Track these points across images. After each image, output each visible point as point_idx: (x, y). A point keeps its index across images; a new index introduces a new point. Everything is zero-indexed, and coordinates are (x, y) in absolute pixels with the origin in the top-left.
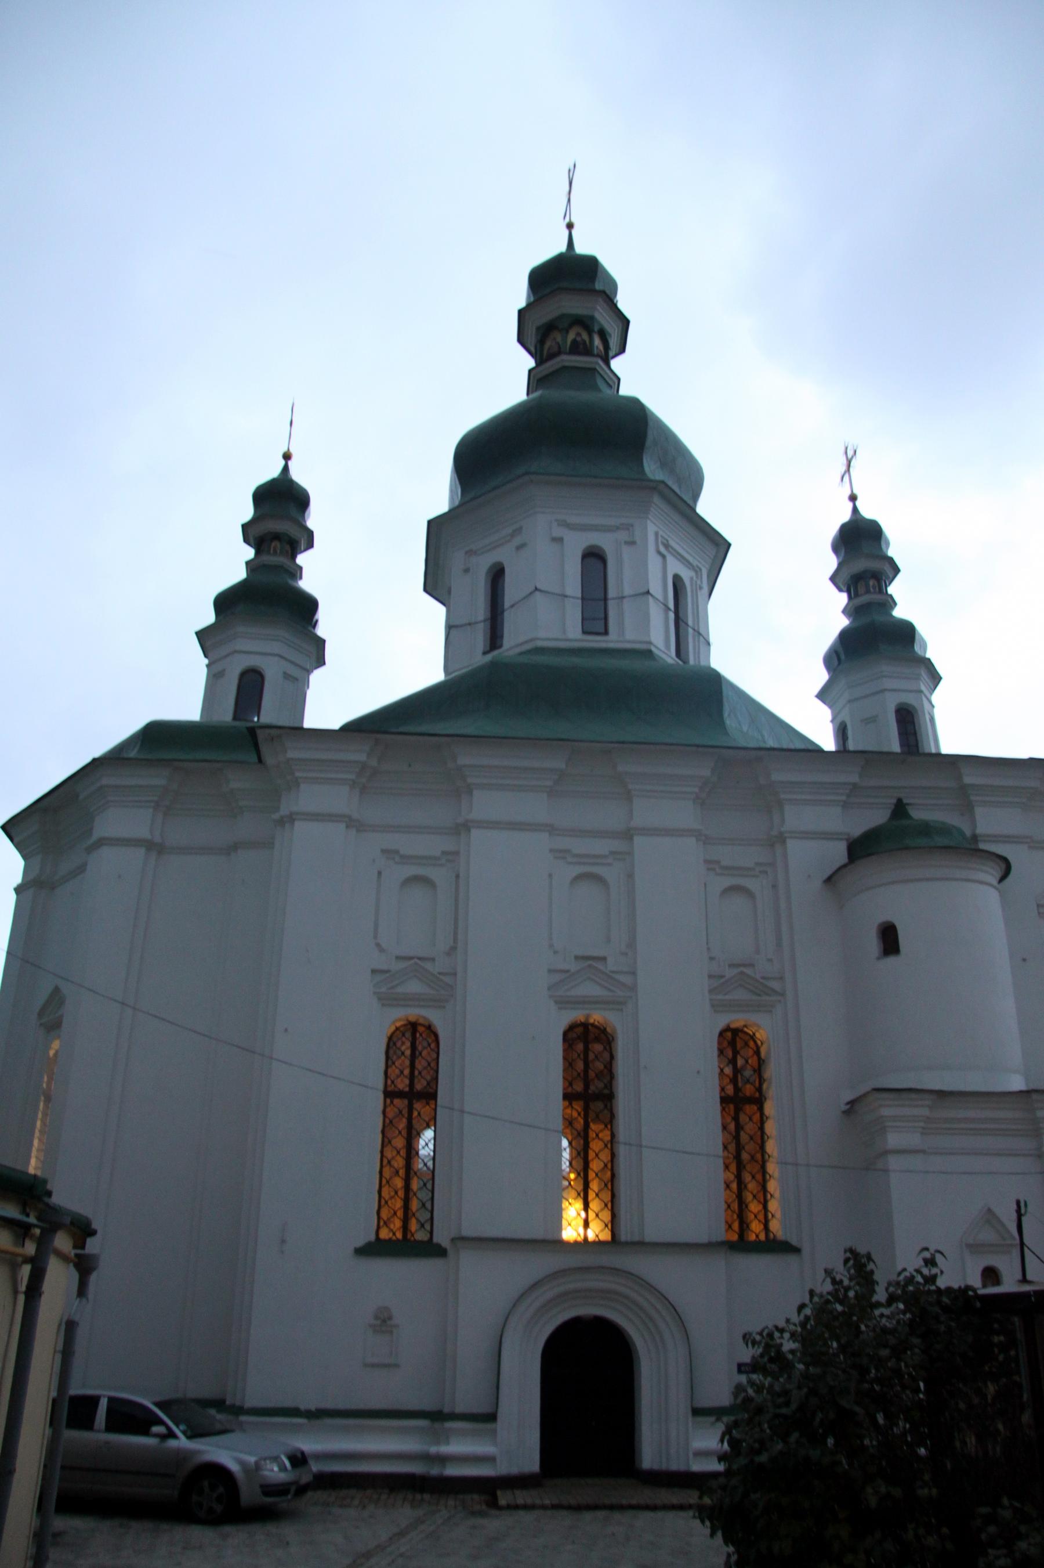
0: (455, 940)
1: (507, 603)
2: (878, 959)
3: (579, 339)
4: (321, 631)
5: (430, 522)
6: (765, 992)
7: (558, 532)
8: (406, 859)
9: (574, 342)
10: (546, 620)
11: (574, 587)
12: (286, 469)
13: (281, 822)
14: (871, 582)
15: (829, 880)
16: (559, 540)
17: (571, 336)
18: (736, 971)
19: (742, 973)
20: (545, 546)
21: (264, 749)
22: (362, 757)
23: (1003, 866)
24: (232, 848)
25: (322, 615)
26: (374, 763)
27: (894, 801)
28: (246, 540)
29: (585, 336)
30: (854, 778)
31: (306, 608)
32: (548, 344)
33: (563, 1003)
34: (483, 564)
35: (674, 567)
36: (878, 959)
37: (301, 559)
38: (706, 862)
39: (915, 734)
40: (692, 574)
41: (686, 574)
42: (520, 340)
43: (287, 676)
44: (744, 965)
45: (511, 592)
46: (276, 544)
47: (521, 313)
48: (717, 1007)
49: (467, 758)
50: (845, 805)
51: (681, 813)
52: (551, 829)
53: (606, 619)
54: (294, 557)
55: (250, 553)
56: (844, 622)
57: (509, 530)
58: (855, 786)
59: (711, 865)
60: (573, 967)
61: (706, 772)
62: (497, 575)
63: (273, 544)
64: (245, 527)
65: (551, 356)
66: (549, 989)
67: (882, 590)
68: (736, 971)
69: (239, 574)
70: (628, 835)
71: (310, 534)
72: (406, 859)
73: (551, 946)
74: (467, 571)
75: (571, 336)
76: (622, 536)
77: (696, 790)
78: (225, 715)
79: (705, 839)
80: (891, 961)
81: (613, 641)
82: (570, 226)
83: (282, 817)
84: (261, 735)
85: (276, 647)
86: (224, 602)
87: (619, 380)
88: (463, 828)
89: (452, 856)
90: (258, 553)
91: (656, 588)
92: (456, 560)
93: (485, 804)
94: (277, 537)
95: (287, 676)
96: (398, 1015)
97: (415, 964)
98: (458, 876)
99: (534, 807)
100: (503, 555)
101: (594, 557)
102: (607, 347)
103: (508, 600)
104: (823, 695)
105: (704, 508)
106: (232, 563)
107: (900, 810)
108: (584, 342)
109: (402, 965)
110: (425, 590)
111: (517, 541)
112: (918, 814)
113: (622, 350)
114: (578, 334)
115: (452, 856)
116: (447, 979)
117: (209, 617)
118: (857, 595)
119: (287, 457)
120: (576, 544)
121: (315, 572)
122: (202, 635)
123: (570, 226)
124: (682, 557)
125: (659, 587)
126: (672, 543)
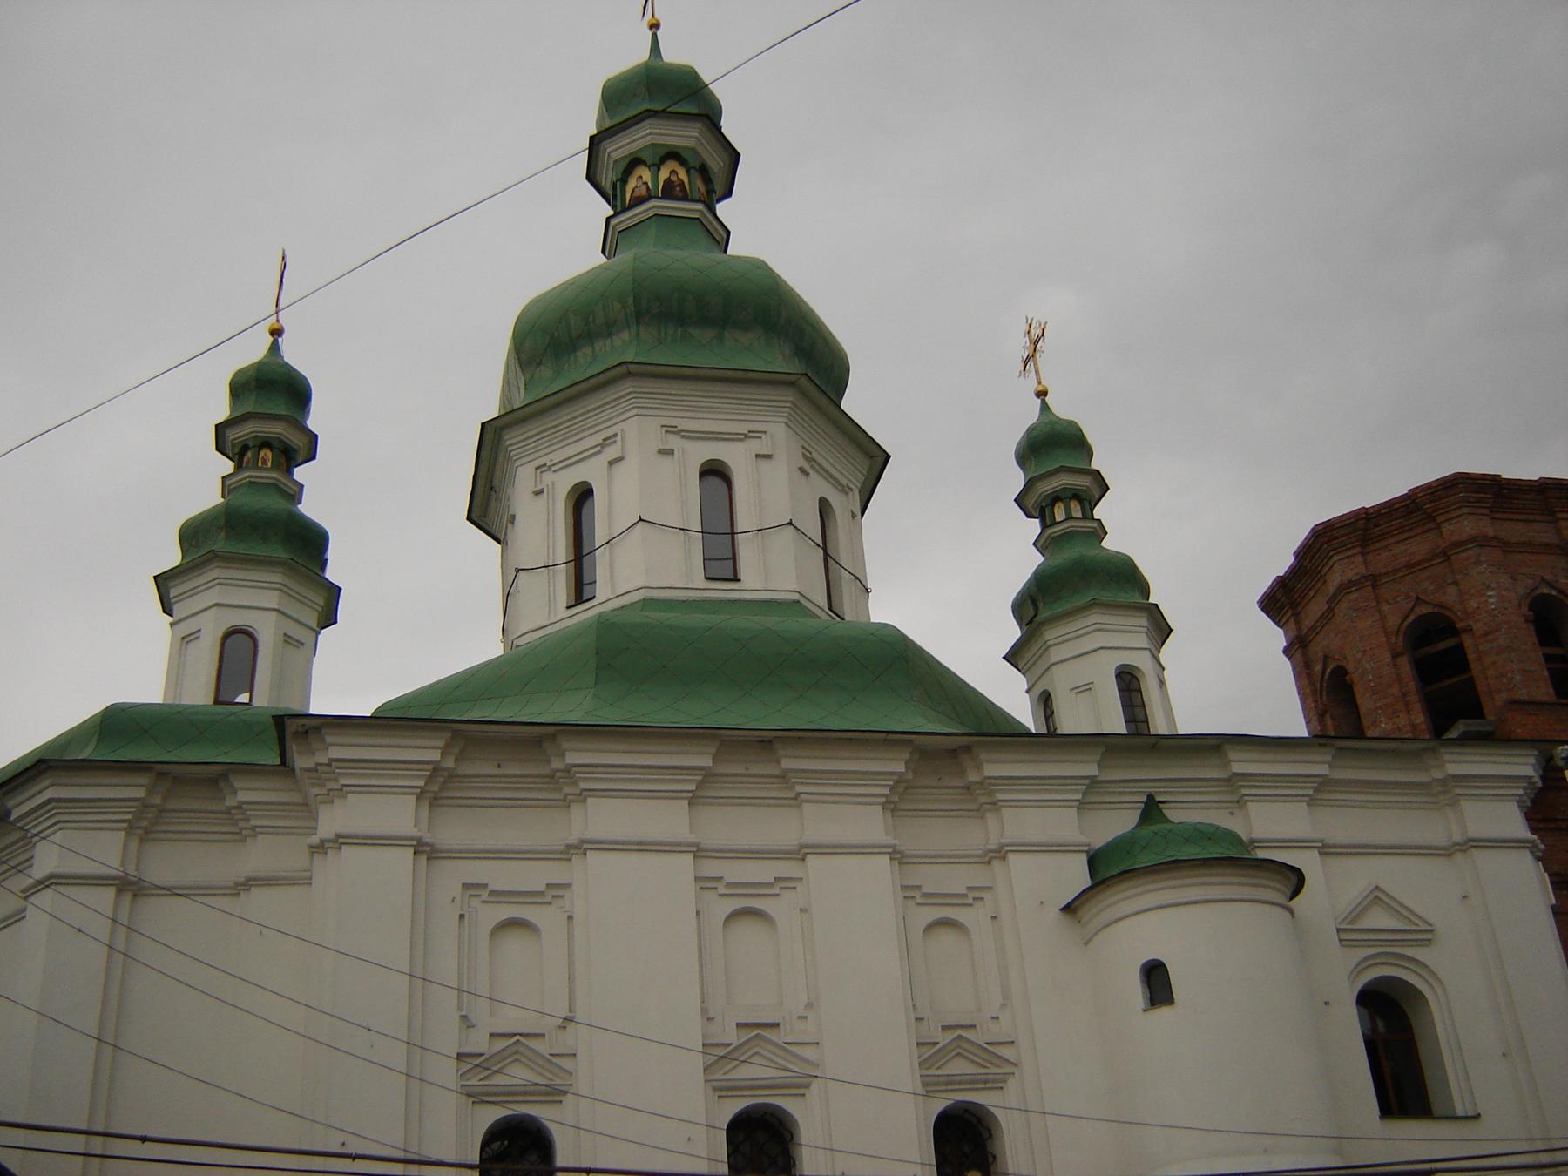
1: (600, 539)
2: (1145, 1011)
3: (674, 178)
4: (331, 574)
5: (483, 425)
6: (995, 1061)
8: (499, 896)
9: (668, 182)
10: (648, 564)
12: (275, 348)
13: (321, 848)
15: (1069, 909)
17: (664, 174)
18: (950, 1036)
19: (960, 1037)
21: (293, 748)
22: (435, 756)
23: (1294, 880)
24: (246, 885)
25: (332, 554)
26: (450, 763)
27: (1144, 799)
28: (220, 448)
29: (682, 174)
30: (1092, 770)
31: (308, 545)
33: (724, 1090)
34: (564, 482)
36: (1145, 1011)
37: (299, 473)
38: (903, 887)
39: (1143, 705)
41: (835, 499)
42: (591, 177)
43: (288, 639)
44: (962, 1027)
45: (603, 521)
46: (266, 454)
47: (592, 138)
48: (930, 1086)
50: (1082, 806)
51: (870, 824)
52: (699, 852)
53: (734, 558)
54: (290, 472)
55: (228, 466)
56: (1037, 559)
57: (598, 439)
58: (1093, 782)
59: (909, 892)
60: (732, 1037)
61: (900, 767)
62: (582, 496)
63: (262, 454)
64: (220, 429)
65: (638, 201)
66: (705, 1070)
67: (1088, 515)
68: (950, 1036)
69: (212, 498)
71: (313, 438)
72: (499, 896)
73: (704, 1011)
74: (539, 493)
75: (664, 174)
77: (887, 791)
78: (199, 693)
79: (899, 857)
80: (1163, 1012)
82: (655, 26)
83: (323, 841)
84: (292, 726)
85: (271, 599)
86: (192, 535)
87: (728, 233)
89: (557, 890)
90: (239, 467)
92: (523, 479)
93: (603, 817)
95: (288, 639)
96: (491, 1115)
97: (516, 1043)
98: (570, 918)
99: (668, 819)
100: (592, 472)
101: (714, 472)
102: (710, 192)
104: (1013, 657)
105: (843, 406)
106: (203, 481)
107: (1151, 810)
109: (501, 1044)
110: (469, 518)
111: (611, 452)
112: (1175, 815)
113: (728, 194)
114: (673, 172)
115: (557, 890)
116: (565, 1063)
118: (1055, 523)
119: (276, 332)
121: (320, 492)
122: (163, 582)
123: (655, 26)
124: (831, 476)
126: (815, 455)
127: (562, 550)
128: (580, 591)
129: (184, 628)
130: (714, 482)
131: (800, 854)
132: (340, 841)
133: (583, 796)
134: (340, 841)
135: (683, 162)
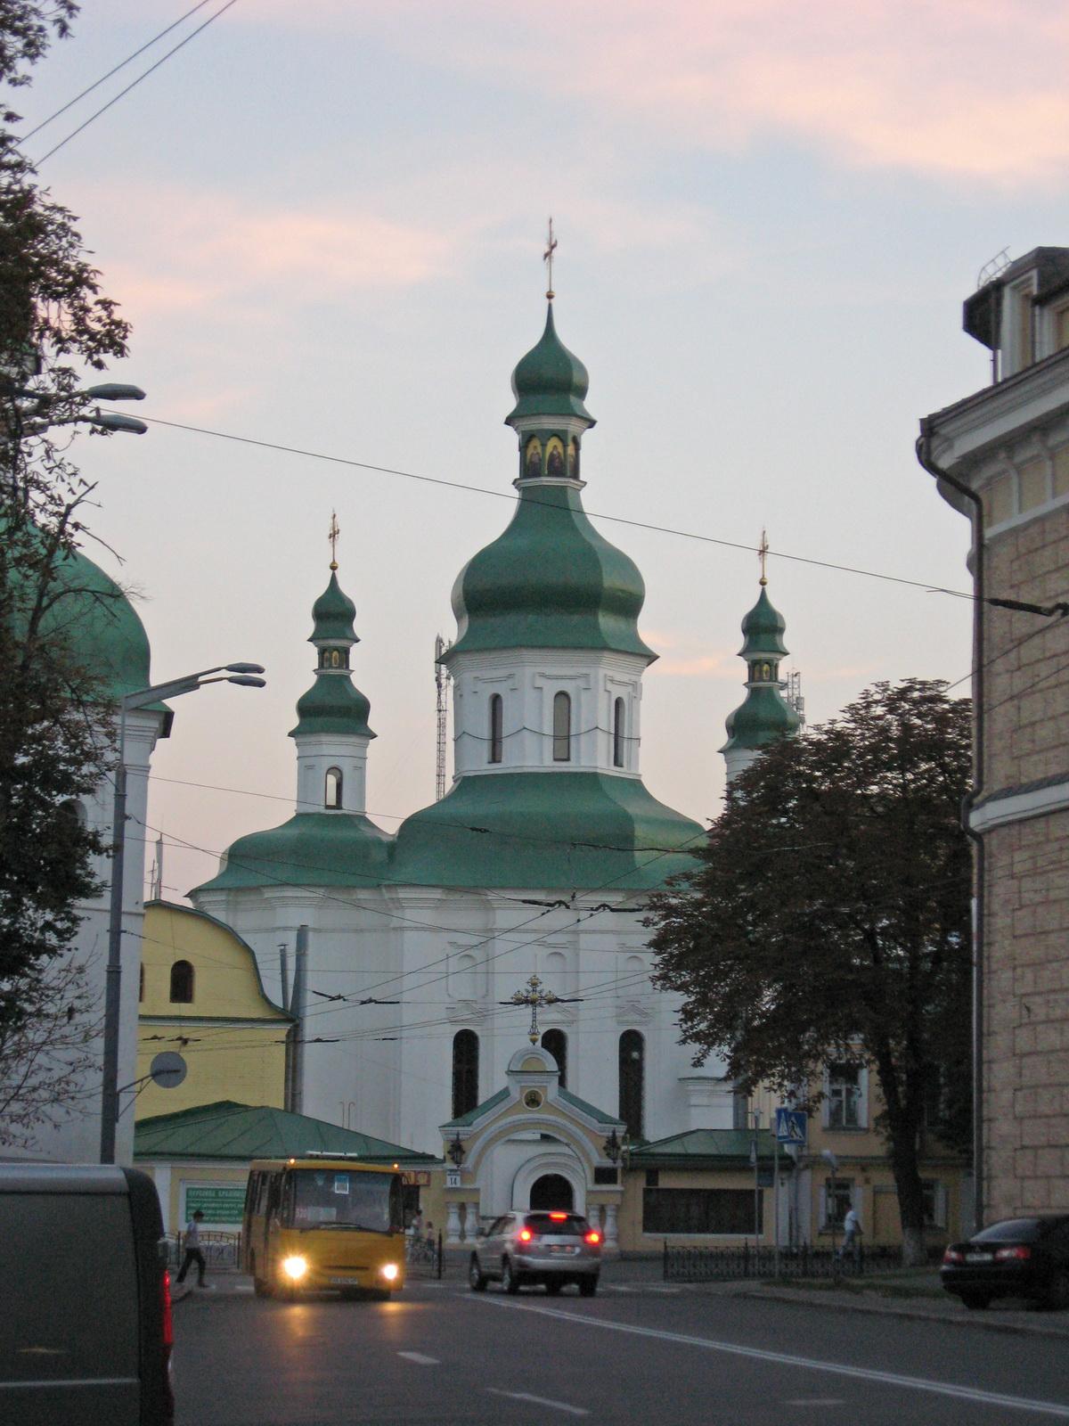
0: (487, 991)
7: (540, 682)
9: (552, 455)
11: (548, 728)
12: (334, 580)
14: (766, 667)
16: (541, 688)
20: (532, 681)
29: (560, 450)
32: (530, 451)
35: (618, 692)
40: (630, 689)
43: (356, 768)
48: (619, 1023)
49: (491, 896)
62: (496, 700)
70: (576, 932)
76: (581, 683)
81: (576, 765)
82: (550, 296)
88: (489, 934)
91: (603, 725)
94: (336, 649)
95: (356, 768)
103: (507, 727)
108: (559, 457)
114: (555, 447)
117: (294, 721)
119: (334, 568)
120: (551, 689)
121: (364, 674)
125: (605, 719)
127: (485, 731)
128: (495, 758)
129: (308, 762)
130: (563, 699)
131: (576, 932)
132: (402, 929)
133: (494, 909)
134: (402, 929)
135: (561, 440)
